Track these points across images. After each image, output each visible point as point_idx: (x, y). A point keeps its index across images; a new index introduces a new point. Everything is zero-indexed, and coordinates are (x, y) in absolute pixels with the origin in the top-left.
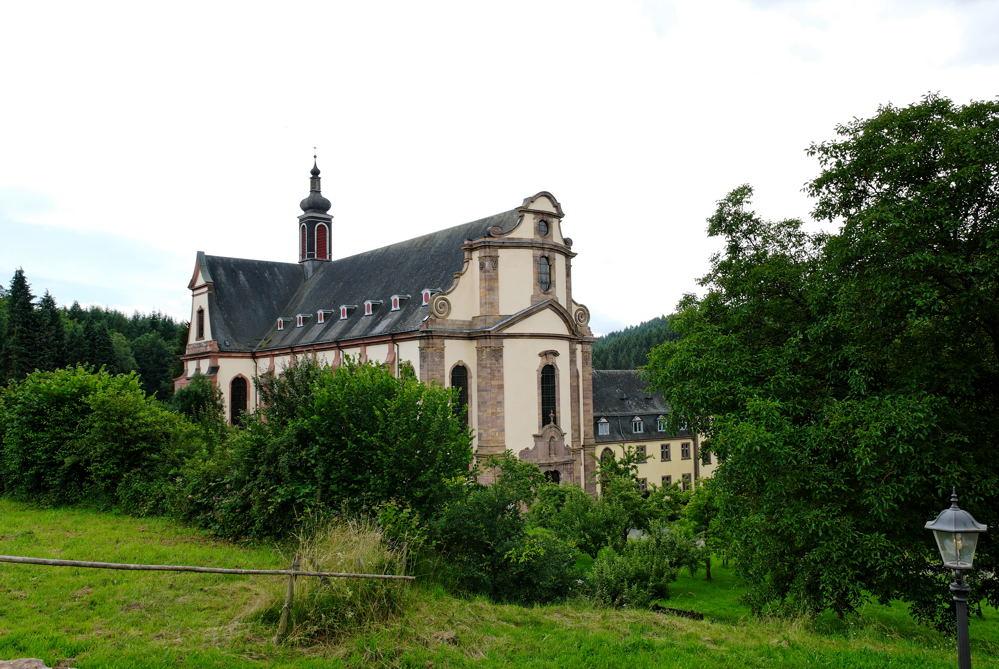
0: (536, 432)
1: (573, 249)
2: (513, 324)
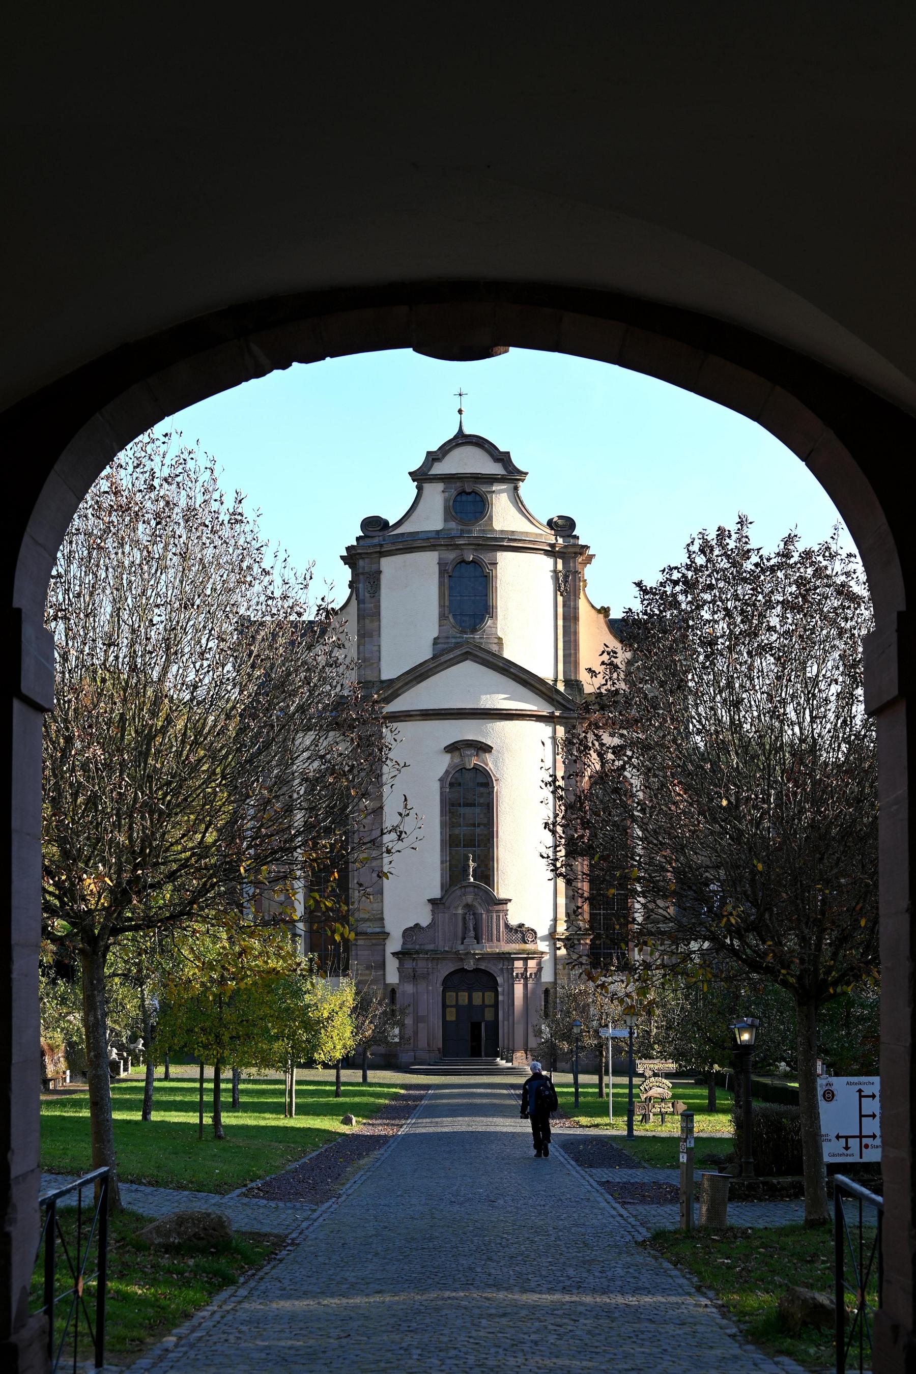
0: (436, 893)
1: (584, 535)
2: (395, 695)
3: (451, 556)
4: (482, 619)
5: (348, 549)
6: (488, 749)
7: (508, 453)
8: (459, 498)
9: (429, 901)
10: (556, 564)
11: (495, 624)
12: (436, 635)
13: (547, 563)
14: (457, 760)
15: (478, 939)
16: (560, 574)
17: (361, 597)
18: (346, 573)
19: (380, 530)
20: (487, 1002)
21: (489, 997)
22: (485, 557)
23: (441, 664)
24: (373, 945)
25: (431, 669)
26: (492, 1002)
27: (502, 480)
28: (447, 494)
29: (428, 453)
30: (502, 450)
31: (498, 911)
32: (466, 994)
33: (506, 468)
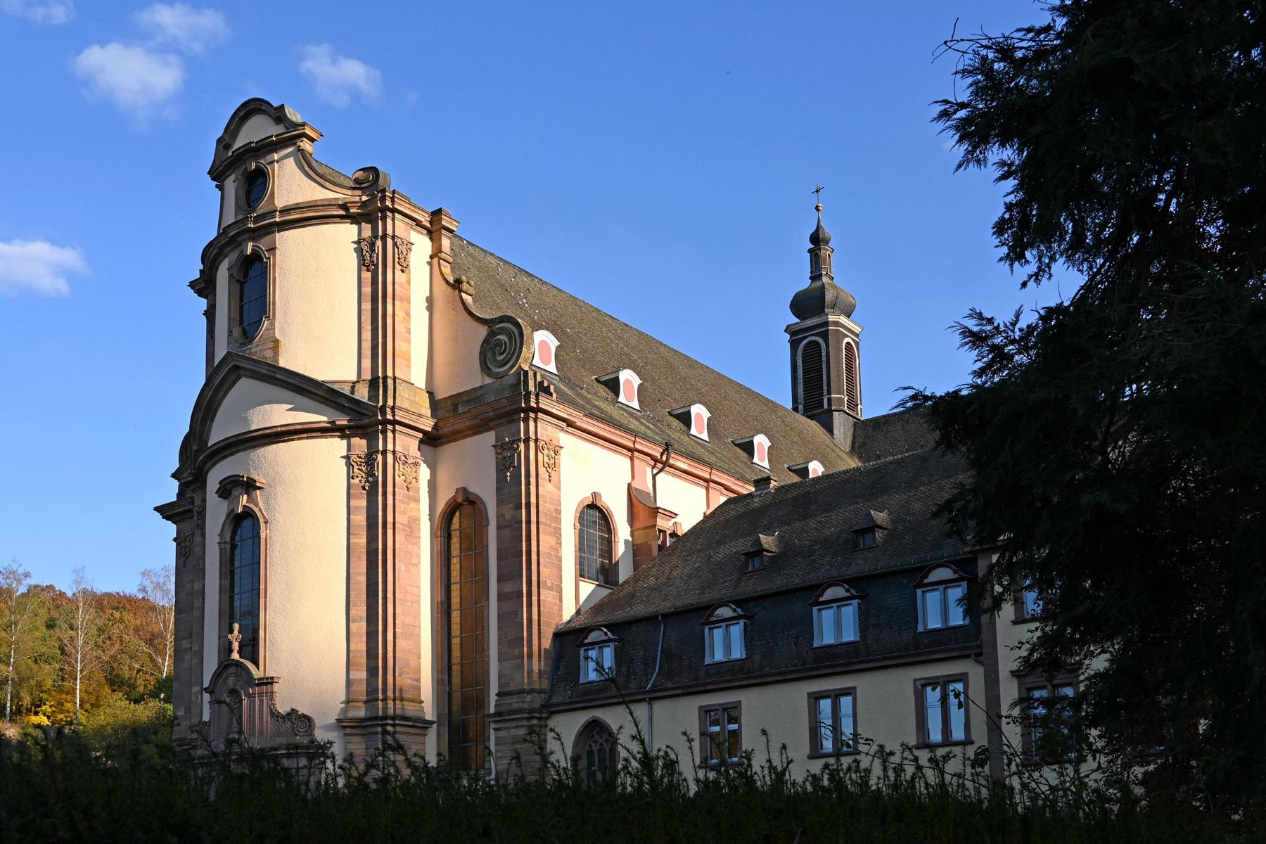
6: (250, 486)
11: (273, 324)
22: (263, 245)
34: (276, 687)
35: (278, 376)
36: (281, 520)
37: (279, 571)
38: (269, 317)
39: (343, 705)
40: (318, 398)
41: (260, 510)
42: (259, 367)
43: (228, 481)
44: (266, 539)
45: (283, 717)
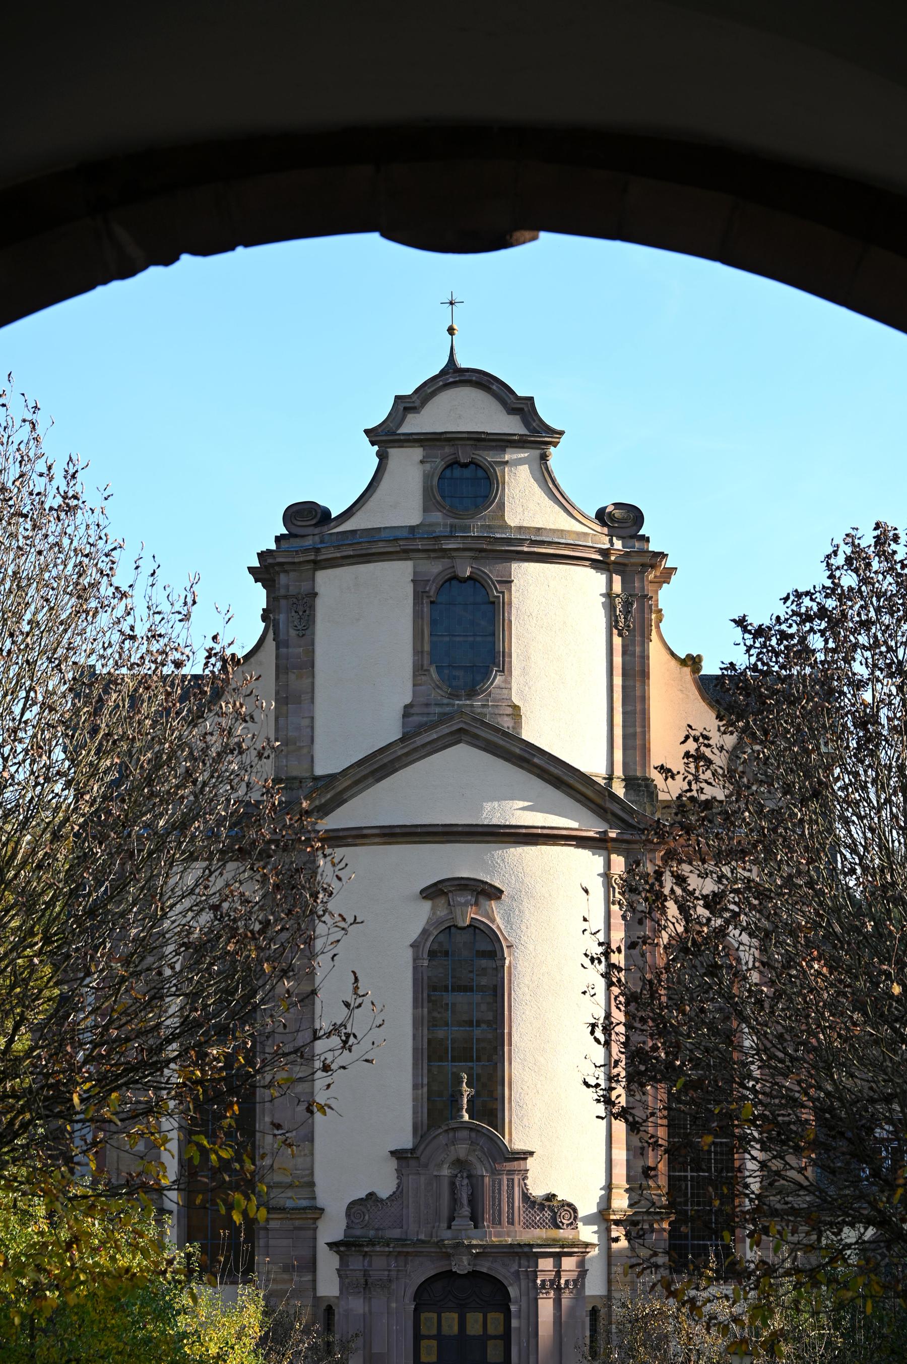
0: (406, 1141)
2: (338, 801)
3: (434, 568)
4: (486, 674)
5: (261, 555)
6: (495, 893)
7: (531, 399)
8: (448, 473)
9: (393, 1153)
10: (610, 582)
11: (508, 682)
12: (408, 700)
13: (596, 581)
14: (442, 912)
15: (476, 1219)
16: (618, 600)
17: (282, 636)
18: (258, 596)
19: (316, 525)
20: (491, 1331)
21: (495, 1319)
22: (492, 571)
23: (415, 750)
24: (296, 1228)
25: (399, 758)
26: (501, 1330)
27: (520, 443)
28: (428, 466)
29: (398, 398)
30: (520, 393)
31: (511, 1172)
32: (456, 1316)
33: (527, 424)
34: (530, 1162)
35: (536, 760)
36: (531, 947)
37: (527, 1013)
38: (503, 671)
39: (603, 1192)
40: (578, 796)
41: (498, 927)
42: (507, 742)
43: (456, 883)
44: (510, 967)
45: (534, 1203)
